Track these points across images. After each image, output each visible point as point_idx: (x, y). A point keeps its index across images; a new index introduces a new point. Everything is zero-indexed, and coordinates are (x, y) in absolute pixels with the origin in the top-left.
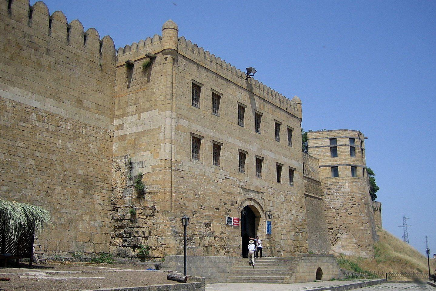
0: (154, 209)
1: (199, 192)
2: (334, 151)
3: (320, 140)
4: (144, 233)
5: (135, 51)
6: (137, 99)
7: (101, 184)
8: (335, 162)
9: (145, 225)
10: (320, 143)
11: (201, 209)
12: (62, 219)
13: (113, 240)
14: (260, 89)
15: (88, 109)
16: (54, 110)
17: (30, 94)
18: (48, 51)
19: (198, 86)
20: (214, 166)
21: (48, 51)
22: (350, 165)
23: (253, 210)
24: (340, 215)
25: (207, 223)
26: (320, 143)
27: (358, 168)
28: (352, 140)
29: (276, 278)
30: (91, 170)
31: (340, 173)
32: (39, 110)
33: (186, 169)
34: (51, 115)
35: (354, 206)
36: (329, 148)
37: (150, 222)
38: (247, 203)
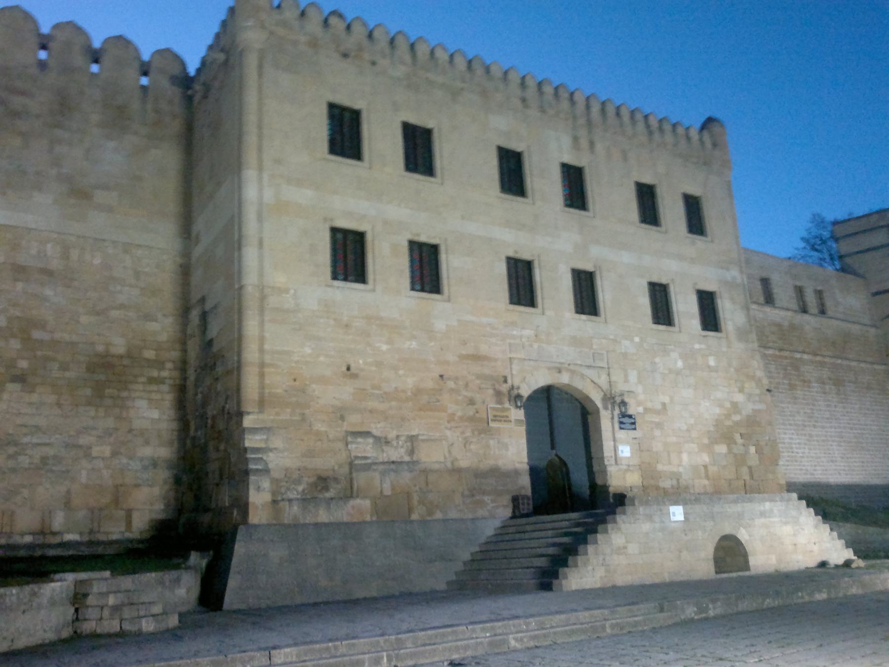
12: (21, 458)
38: (541, 379)
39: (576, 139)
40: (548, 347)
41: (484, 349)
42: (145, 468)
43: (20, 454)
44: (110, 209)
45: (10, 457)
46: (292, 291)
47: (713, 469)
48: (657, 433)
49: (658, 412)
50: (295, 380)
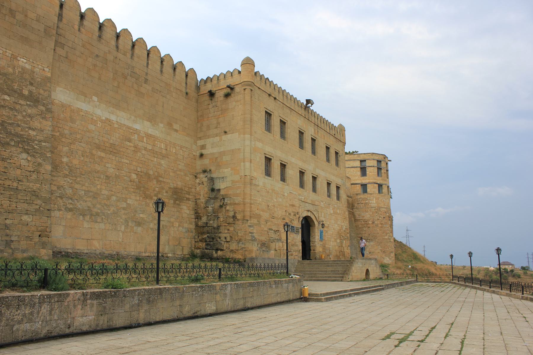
0: (234, 217)
1: (271, 204)
4: (226, 238)
5: (216, 82)
6: (218, 123)
7: (187, 196)
9: (226, 231)
10: (352, 164)
13: (196, 244)
14: (315, 117)
15: (176, 131)
16: (151, 131)
19: (269, 113)
20: (281, 182)
21: (146, 81)
22: (377, 183)
23: (309, 220)
24: (368, 226)
26: (352, 164)
27: (384, 186)
28: (379, 162)
29: (335, 277)
30: (179, 183)
31: (368, 190)
33: (261, 184)
34: (149, 136)
36: (359, 169)
38: (305, 214)
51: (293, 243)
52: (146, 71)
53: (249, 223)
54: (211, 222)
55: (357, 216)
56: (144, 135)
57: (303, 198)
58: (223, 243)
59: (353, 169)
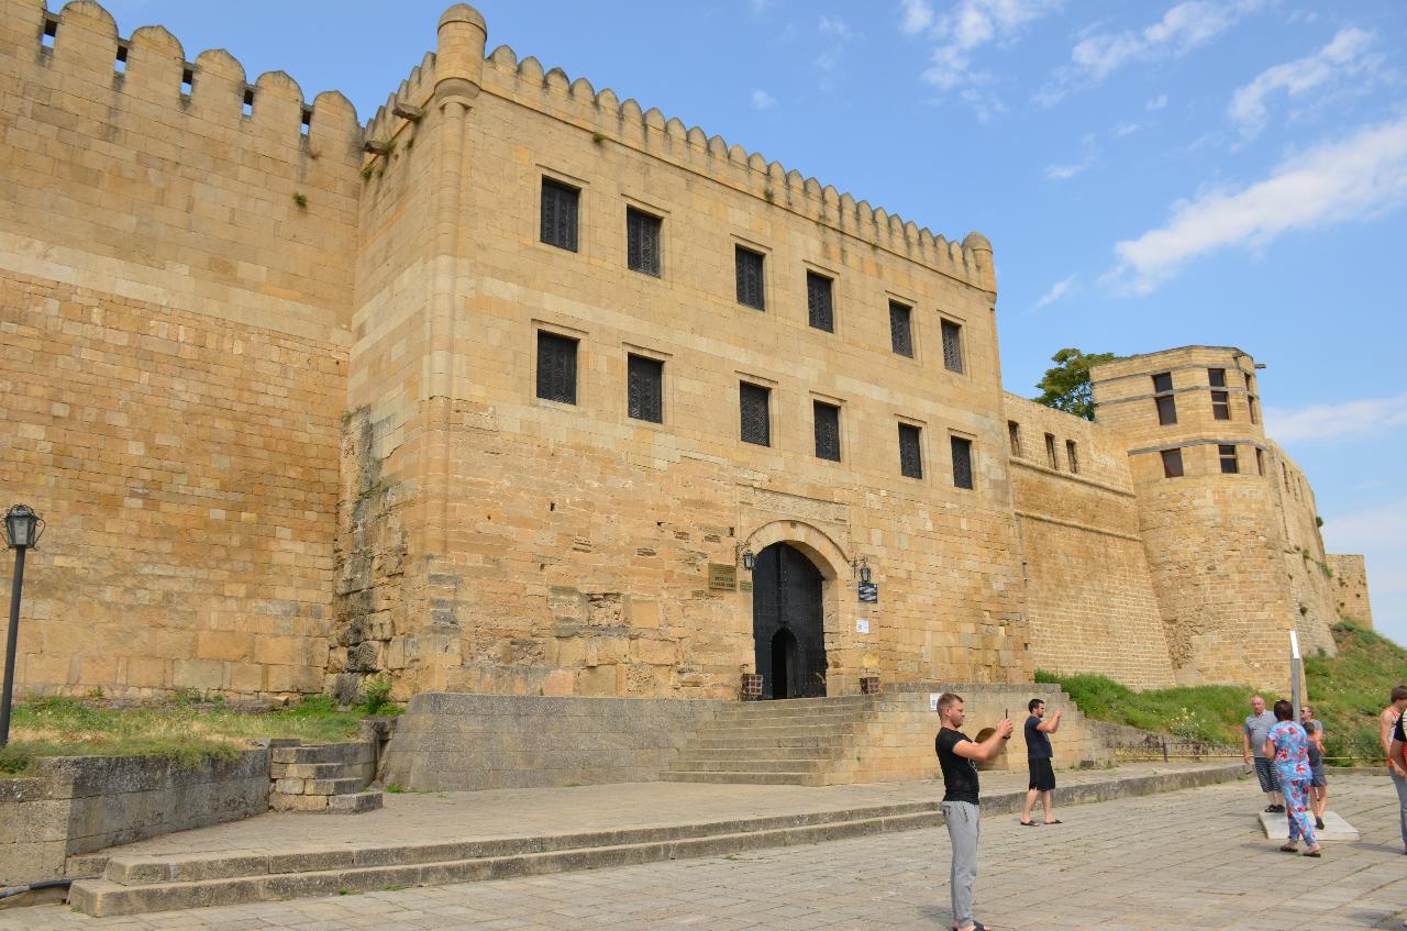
2: (1166, 409)
3: (1125, 381)
8: (1171, 437)
9: (384, 604)
10: (1126, 389)
11: (575, 549)
12: (140, 593)
13: (333, 654)
16: (124, 288)
17: (38, 245)
18: (111, 132)
21: (111, 132)
22: (1214, 442)
23: (810, 557)
25: (605, 595)
31: (1186, 466)
32: (73, 289)
35: (1235, 553)
36: (1152, 403)
37: (395, 594)
38: (775, 535)
39: (825, 246)
40: (779, 493)
41: (708, 494)
42: (286, 614)
43: (140, 588)
44: (256, 287)
45: (127, 590)
46: (491, 409)
47: (959, 652)
48: (899, 605)
49: (902, 582)
50: (489, 518)
51: (704, 639)
52: (111, 102)
53: (435, 567)
54: (359, 576)
55: (1157, 553)
56: (94, 302)
57: (759, 476)
58: (375, 644)
59: (1132, 405)
